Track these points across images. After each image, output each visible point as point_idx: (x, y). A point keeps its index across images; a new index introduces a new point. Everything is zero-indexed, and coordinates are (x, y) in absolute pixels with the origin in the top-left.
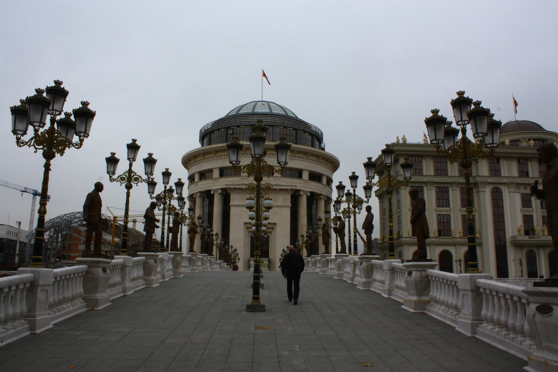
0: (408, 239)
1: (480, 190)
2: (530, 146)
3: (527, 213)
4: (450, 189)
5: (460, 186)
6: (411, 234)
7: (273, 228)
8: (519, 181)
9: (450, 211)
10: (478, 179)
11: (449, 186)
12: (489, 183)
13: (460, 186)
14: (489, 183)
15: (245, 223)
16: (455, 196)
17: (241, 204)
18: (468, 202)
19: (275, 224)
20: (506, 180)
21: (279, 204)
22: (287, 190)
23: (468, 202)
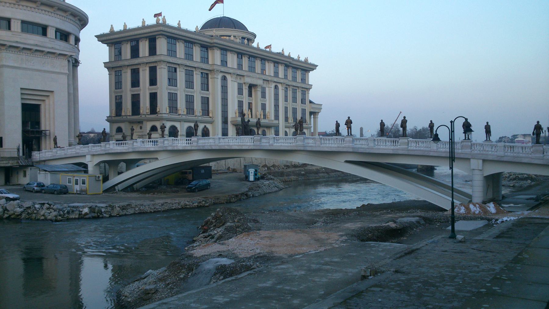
0: (167, 115)
1: (215, 76)
2: (243, 43)
3: (240, 100)
4: (195, 73)
5: (168, 65)
6: (168, 110)
7: (48, 96)
8: (239, 72)
9: (194, 92)
10: (215, 67)
11: (194, 70)
12: (221, 72)
13: (168, 65)
14: (221, 72)
15: (21, 89)
16: (197, 79)
17: (16, 65)
18: (205, 86)
19: (52, 92)
20: (231, 71)
21: (57, 70)
22: (65, 55)
23: (205, 86)
